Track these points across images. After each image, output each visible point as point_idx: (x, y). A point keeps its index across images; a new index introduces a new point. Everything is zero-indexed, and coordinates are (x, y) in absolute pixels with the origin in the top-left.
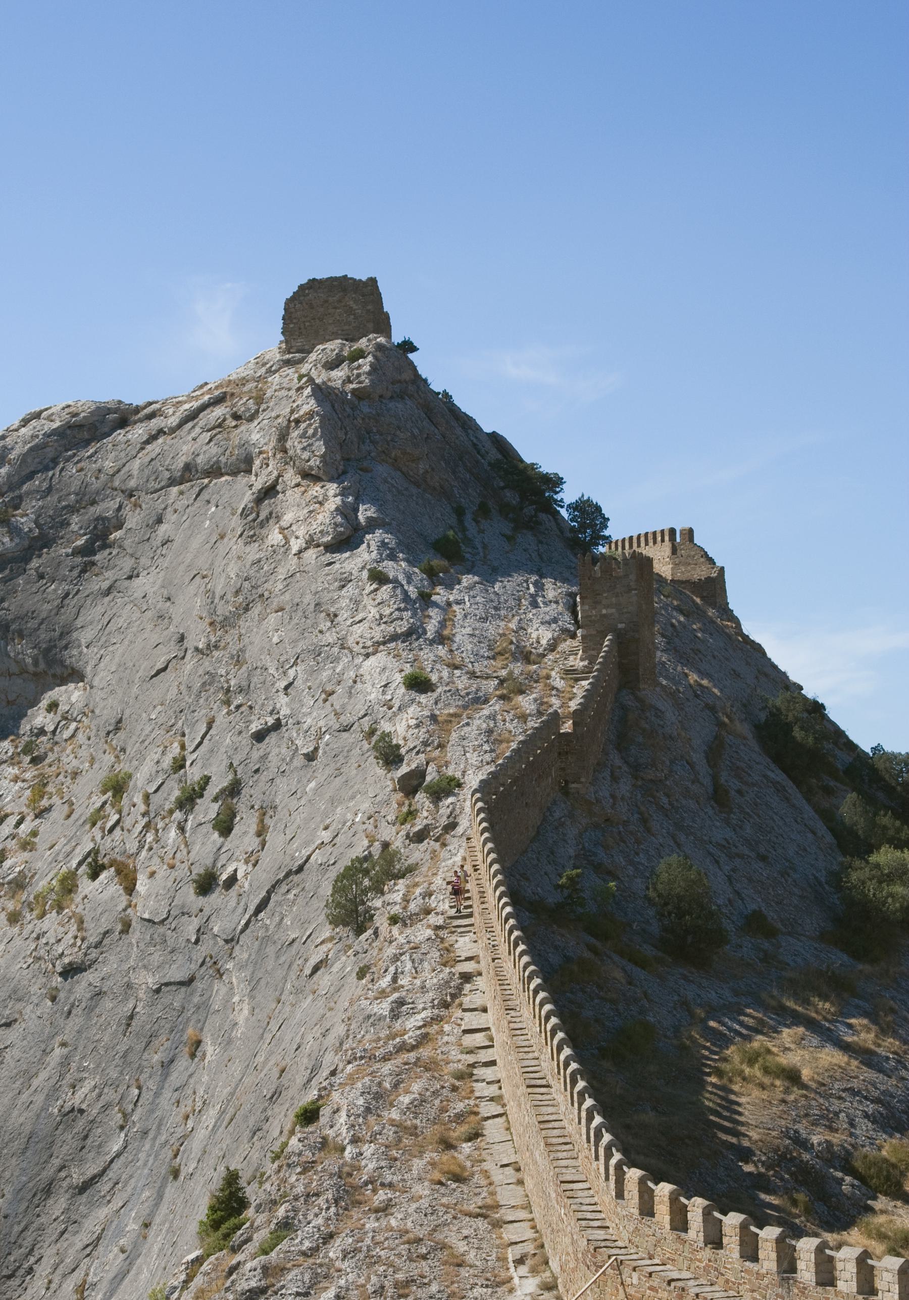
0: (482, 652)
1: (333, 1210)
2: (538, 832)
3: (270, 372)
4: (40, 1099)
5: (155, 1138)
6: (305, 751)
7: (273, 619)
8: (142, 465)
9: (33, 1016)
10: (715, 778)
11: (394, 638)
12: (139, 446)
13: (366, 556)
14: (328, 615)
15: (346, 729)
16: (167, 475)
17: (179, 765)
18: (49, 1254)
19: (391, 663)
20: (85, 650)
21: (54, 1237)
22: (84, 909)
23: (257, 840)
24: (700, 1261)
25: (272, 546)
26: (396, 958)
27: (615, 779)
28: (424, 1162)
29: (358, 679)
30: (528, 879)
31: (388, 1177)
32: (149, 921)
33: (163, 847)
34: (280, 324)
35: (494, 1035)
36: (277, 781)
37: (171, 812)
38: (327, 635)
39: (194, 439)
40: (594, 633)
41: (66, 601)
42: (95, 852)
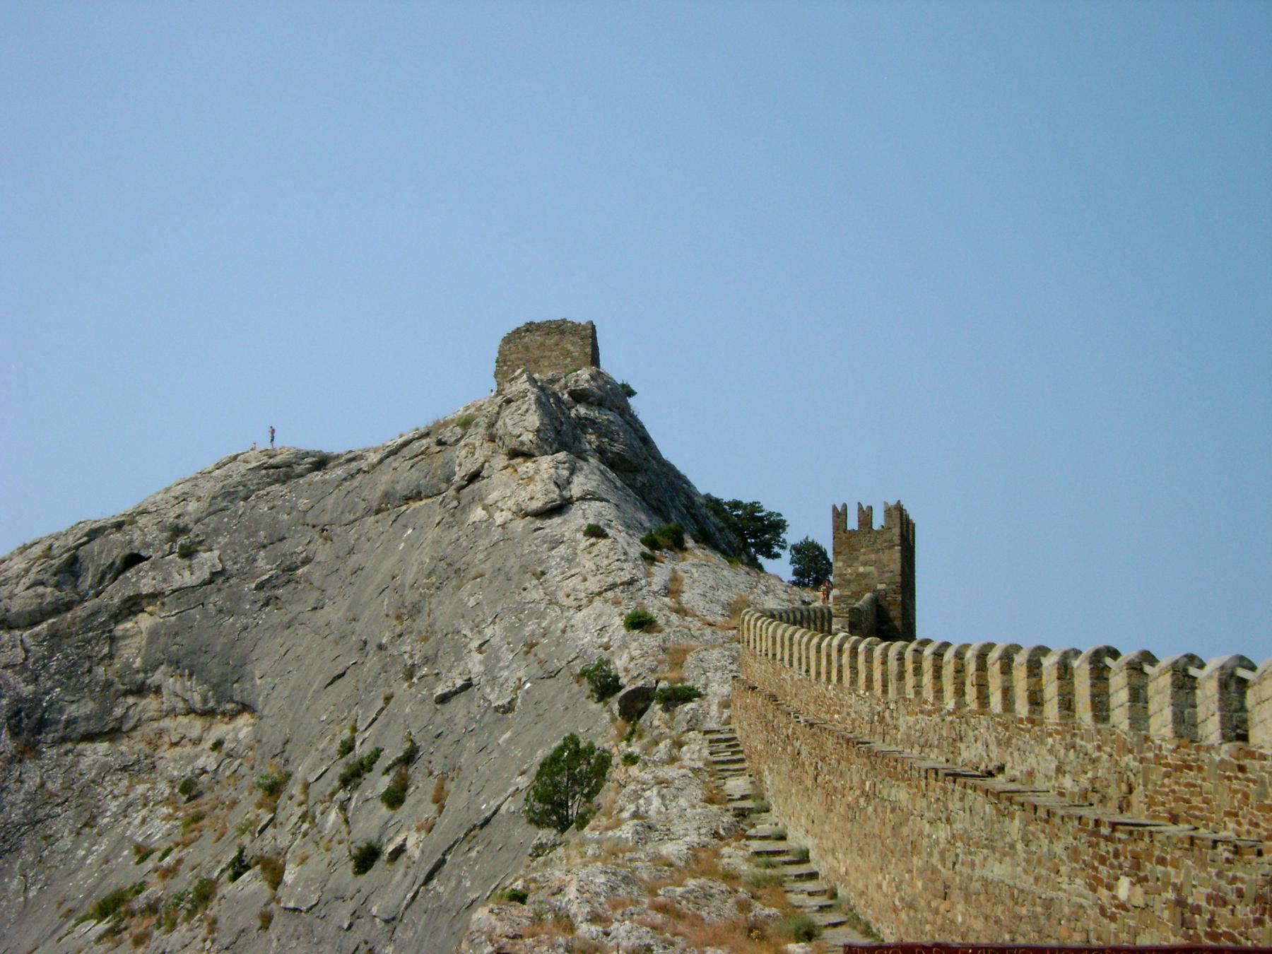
6: (500, 703)
11: (612, 587)
13: (583, 521)
16: (363, 505)
17: (348, 748)
19: (609, 608)
20: (258, 682)
22: (219, 911)
23: (435, 807)
29: (568, 629)
32: (295, 910)
34: (493, 367)
36: (464, 742)
37: (333, 794)
39: (395, 469)
40: (849, 593)
41: (244, 634)
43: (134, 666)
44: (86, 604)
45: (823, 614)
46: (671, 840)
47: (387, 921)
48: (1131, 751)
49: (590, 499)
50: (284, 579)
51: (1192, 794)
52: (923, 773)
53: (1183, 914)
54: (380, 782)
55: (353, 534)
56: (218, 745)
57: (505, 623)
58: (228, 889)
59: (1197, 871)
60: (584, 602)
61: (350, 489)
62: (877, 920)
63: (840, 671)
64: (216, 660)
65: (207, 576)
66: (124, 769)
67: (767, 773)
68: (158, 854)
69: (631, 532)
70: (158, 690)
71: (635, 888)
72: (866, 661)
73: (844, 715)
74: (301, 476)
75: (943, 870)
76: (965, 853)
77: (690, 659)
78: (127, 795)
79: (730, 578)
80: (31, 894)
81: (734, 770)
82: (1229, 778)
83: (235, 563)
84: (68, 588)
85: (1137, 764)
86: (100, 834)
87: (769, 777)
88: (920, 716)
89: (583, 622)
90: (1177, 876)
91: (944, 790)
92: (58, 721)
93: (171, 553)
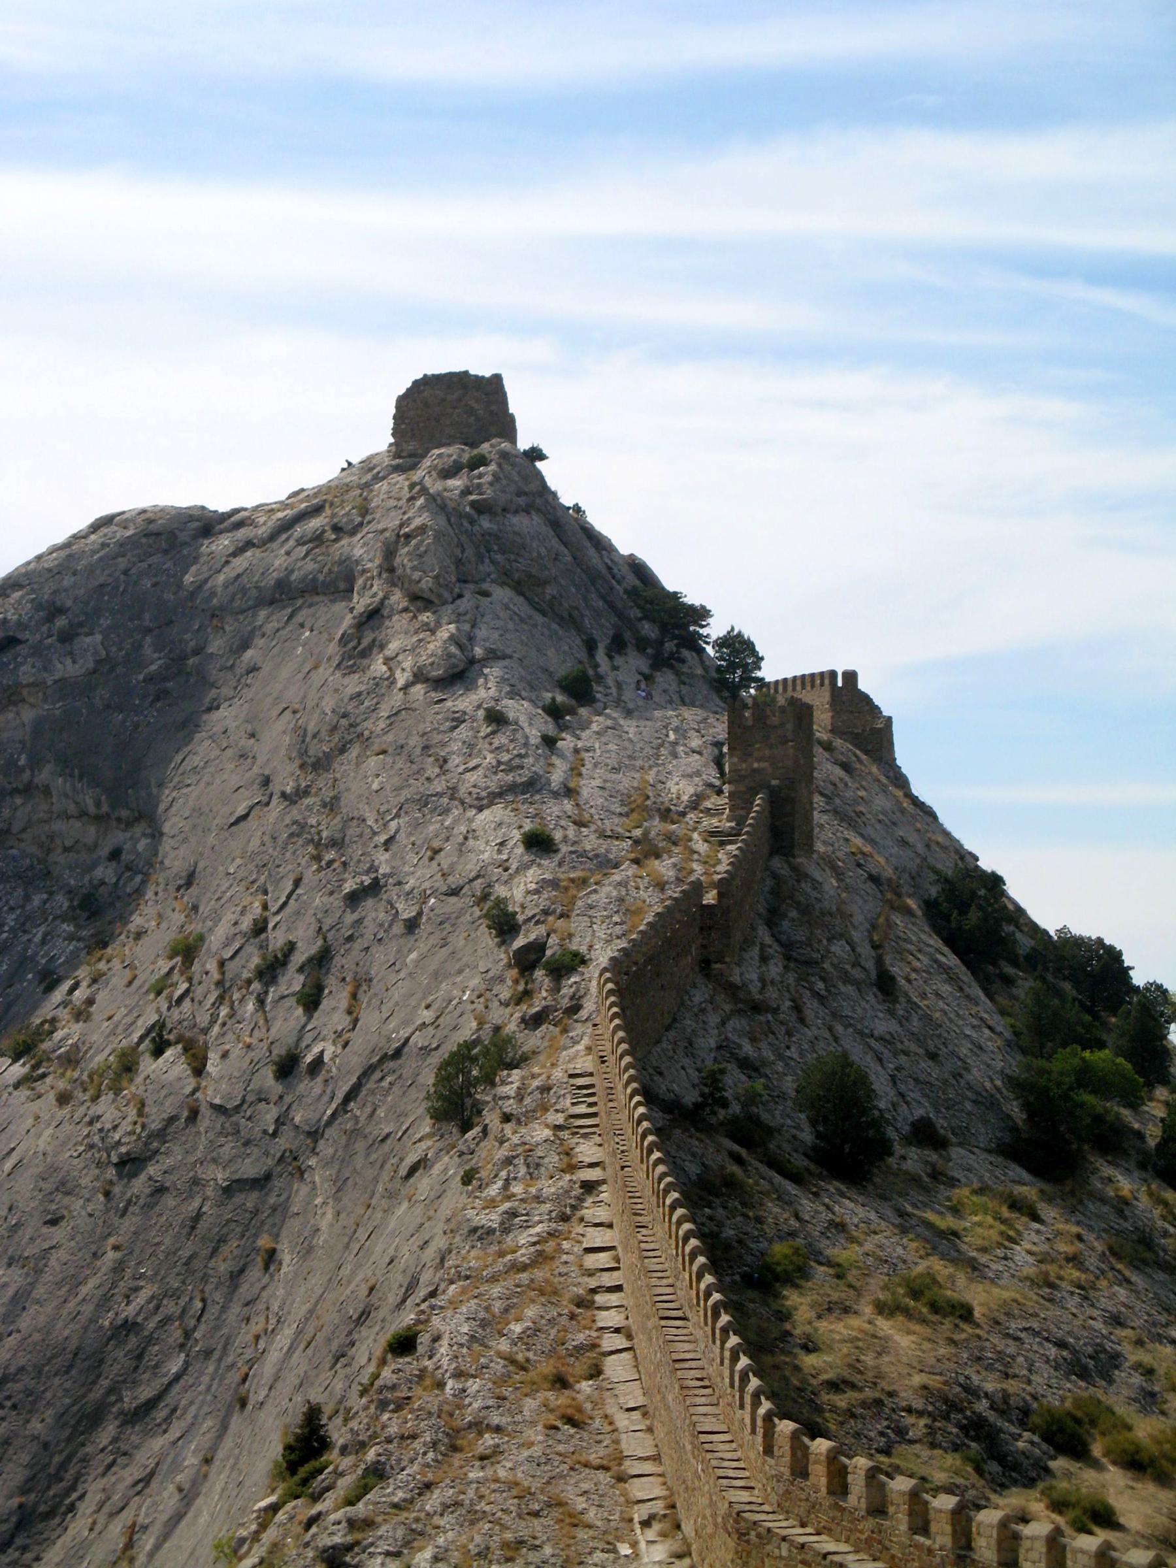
0: (613, 808)
1: (431, 1455)
2: (675, 1020)
3: (377, 478)
4: (88, 1309)
5: (220, 1360)
6: (406, 916)
7: (373, 762)
9: (83, 1213)
10: (879, 962)
11: (512, 788)
12: (224, 559)
15: (455, 892)
16: (254, 593)
18: (94, 1488)
21: (100, 1470)
23: (348, 1019)
24: (861, 1532)
25: (374, 678)
26: (508, 1161)
27: (764, 959)
28: (537, 1402)
29: (470, 836)
30: (661, 1074)
31: (495, 1420)
32: (220, 1107)
33: (239, 1022)
35: (621, 1255)
36: (373, 950)
37: (249, 982)
38: (435, 782)
40: (743, 789)
42: (160, 1025)
43: (20, 763)
54: (292, 981)
56: (115, 855)
58: (149, 1066)
61: (240, 570)
66: (19, 876)
78: (23, 907)
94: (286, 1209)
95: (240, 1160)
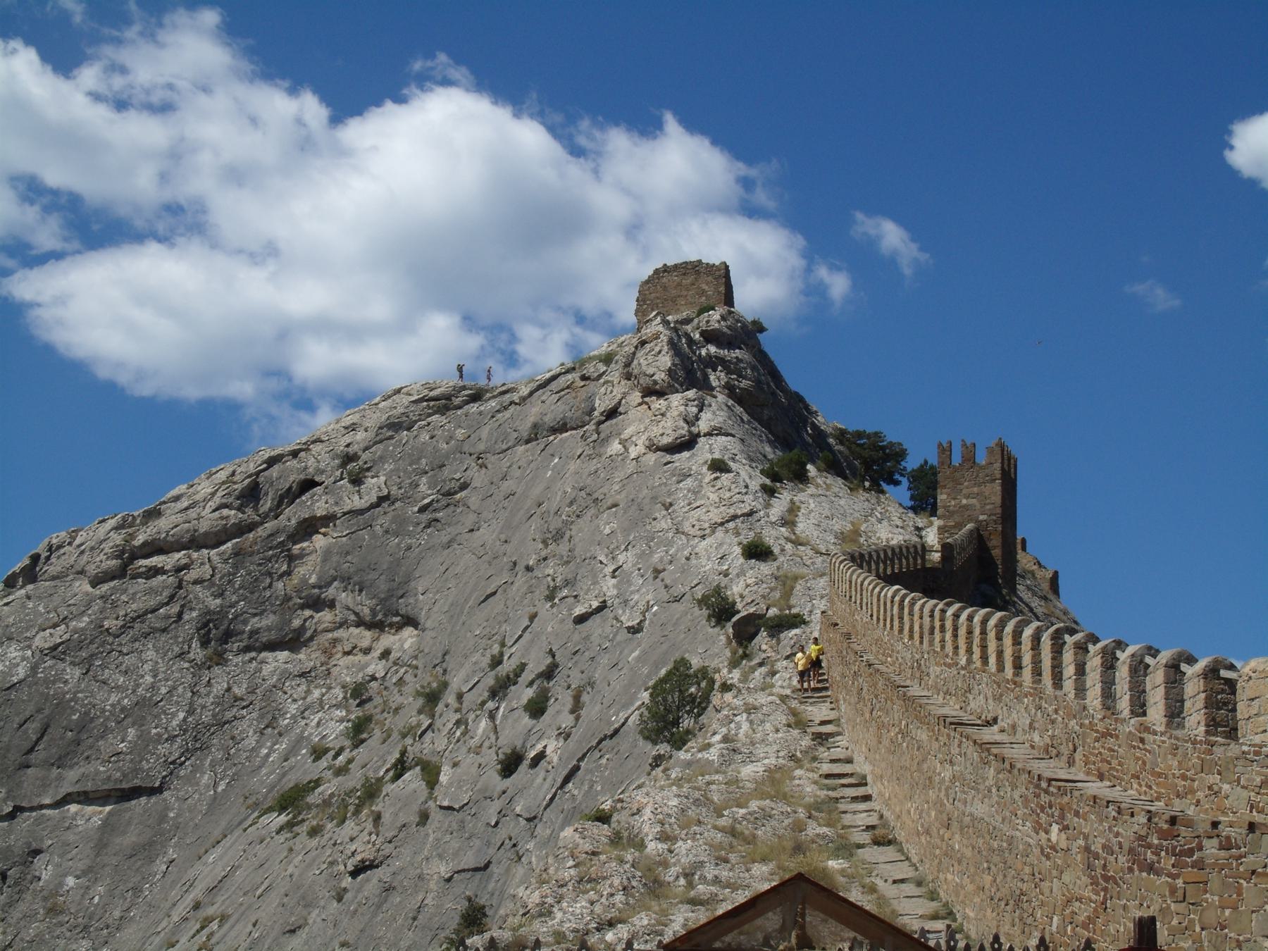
6: (630, 624)
8: (491, 429)
9: (319, 920)
11: (734, 517)
14: (663, 505)
16: (515, 435)
17: (496, 662)
20: (421, 597)
23: (572, 717)
25: (611, 456)
29: (693, 557)
32: (450, 808)
36: (598, 659)
37: (483, 703)
39: (543, 402)
41: (408, 554)
42: (403, 753)
44: (266, 525)
45: (916, 552)
46: (752, 762)
47: (529, 820)
48: (1075, 717)
49: (717, 435)
50: (444, 503)
51: (1112, 757)
52: (936, 720)
53: (1088, 858)
55: (505, 463)
56: (386, 654)
57: (637, 550)
59: (1097, 825)
60: (707, 531)
62: (907, 841)
63: (892, 620)
64: (383, 577)
65: (374, 499)
66: (302, 675)
67: (842, 702)
68: (332, 753)
69: (754, 465)
70: (331, 605)
71: (704, 810)
72: (909, 614)
73: (895, 658)
74: (460, 407)
75: (948, 804)
76: (961, 792)
77: (799, 587)
78: (304, 698)
79: (846, 507)
80: (220, 789)
81: (818, 698)
82: (1134, 747)
83: (400, 488)
84: (249, 511)
85: (1078, 728)
86: (280, 734)
87: (843, 706)
88: (944, 667)
89: (706, 550)
90: (1086, 828)
91: (948, 735)
92: (244, 632)
93: (342, 479)
94: (502, 892)
95: (463, 853)
